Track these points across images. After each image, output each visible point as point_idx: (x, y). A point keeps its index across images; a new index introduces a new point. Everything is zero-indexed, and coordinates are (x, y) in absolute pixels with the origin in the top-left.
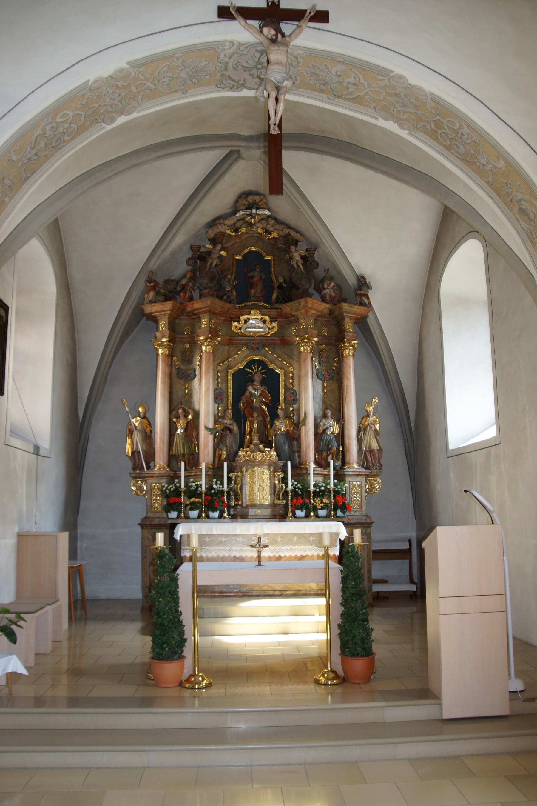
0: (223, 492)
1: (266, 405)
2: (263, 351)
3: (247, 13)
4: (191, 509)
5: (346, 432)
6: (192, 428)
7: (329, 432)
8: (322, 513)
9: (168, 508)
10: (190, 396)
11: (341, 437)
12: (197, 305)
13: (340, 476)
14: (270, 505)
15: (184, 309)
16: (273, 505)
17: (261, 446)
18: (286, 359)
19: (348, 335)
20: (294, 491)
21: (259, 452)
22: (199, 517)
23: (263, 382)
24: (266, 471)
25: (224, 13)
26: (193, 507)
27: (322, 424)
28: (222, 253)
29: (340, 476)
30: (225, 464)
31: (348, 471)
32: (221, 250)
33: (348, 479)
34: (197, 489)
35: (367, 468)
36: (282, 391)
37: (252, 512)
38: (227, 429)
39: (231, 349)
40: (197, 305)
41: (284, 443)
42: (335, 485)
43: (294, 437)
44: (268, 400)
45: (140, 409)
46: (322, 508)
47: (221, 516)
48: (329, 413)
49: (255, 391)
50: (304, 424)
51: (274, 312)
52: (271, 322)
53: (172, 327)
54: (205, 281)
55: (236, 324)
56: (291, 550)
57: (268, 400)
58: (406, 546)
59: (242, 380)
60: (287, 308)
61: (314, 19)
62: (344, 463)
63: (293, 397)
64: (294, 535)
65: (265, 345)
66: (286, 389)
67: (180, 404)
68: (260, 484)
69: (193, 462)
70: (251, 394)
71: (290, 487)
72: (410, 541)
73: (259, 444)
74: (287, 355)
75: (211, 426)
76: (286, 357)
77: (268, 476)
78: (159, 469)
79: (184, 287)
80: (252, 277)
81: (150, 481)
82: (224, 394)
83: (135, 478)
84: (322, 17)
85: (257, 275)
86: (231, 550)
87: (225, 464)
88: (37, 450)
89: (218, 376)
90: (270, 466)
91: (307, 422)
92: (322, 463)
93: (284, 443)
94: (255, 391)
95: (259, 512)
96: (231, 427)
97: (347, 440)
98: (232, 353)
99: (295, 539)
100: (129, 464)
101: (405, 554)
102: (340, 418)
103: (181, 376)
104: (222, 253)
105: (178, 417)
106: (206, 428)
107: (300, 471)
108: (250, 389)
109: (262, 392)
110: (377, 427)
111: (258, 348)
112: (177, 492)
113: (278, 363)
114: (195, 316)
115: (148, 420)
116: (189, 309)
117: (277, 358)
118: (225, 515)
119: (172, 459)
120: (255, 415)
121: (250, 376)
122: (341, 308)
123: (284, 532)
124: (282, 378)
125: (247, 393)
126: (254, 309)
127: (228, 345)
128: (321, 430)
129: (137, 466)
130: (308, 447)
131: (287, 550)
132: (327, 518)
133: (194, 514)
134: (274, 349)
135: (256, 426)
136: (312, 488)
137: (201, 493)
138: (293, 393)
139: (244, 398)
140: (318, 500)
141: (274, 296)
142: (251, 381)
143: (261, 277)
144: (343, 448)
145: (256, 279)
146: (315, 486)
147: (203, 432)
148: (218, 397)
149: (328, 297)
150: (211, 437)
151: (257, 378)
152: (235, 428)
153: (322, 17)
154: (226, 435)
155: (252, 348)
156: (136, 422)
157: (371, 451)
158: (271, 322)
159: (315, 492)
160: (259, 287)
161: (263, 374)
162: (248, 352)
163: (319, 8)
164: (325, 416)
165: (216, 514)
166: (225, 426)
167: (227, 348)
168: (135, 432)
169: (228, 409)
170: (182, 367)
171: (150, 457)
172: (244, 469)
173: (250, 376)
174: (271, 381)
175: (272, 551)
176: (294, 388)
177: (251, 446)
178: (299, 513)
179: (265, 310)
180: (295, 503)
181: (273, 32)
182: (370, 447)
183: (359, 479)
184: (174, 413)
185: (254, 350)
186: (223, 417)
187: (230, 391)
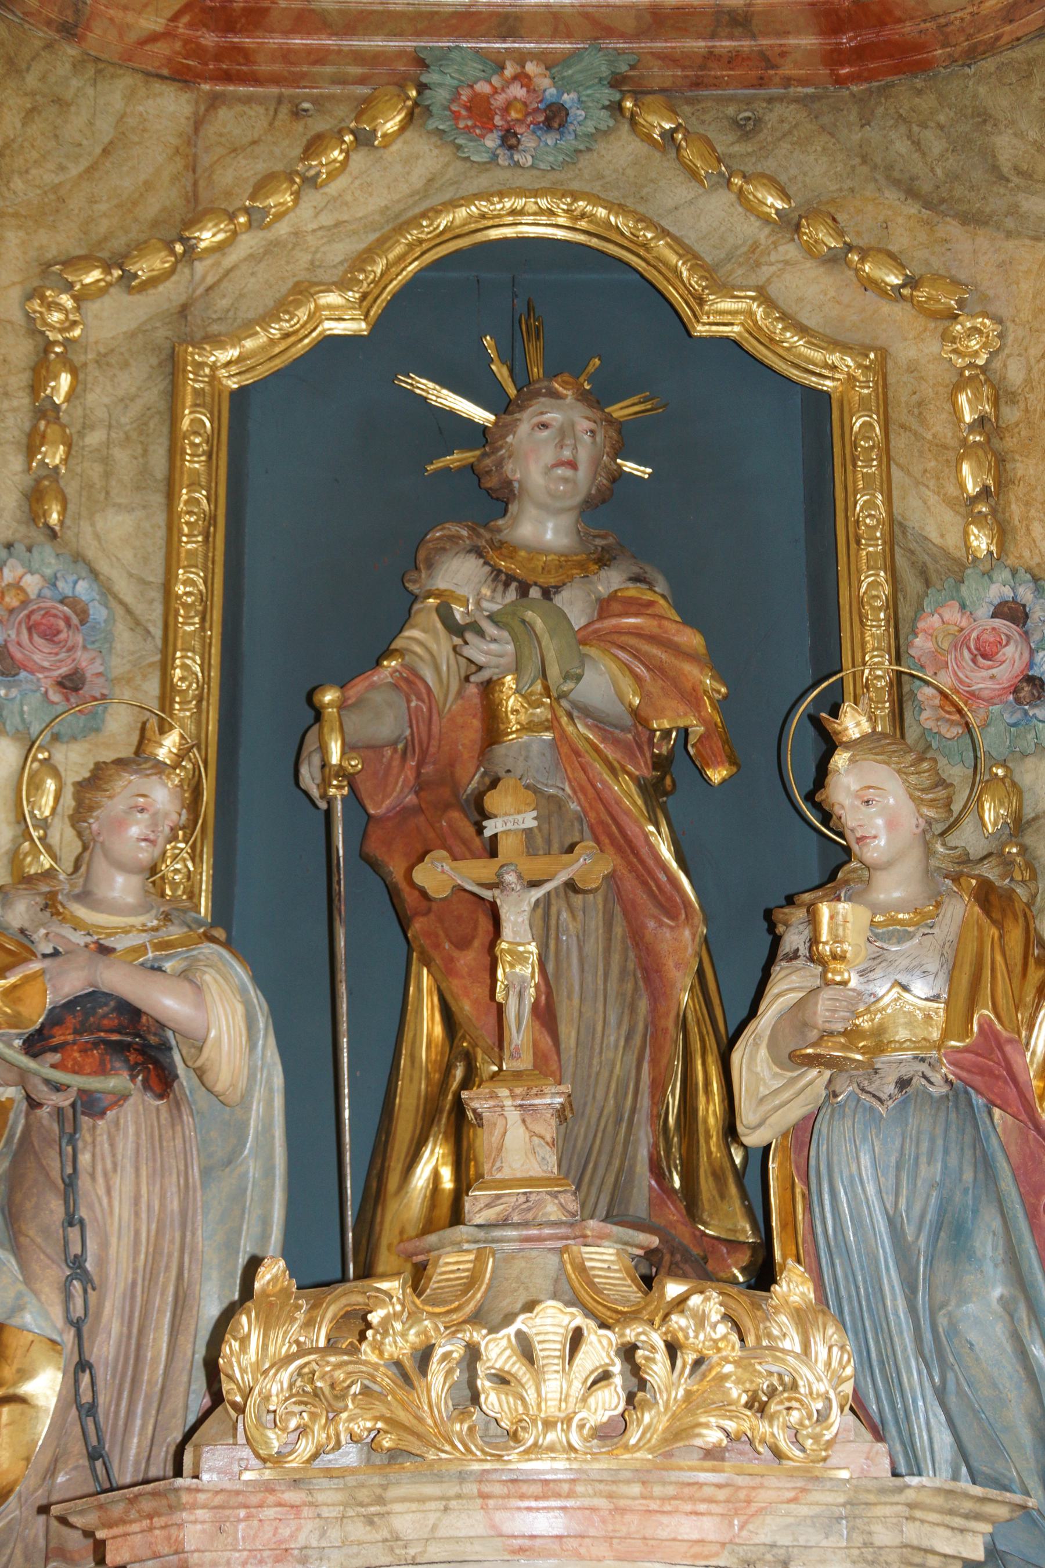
1: (666, 777)
18: (899, 242)
21: (551, 1321)
36: (870, 583)
39: (227, 122)
41: (953, 1233)
44: (692, 698)
49: (523, 651)
57: (692, 698)
63: (1013, 655)
73: (573, 1228)
74: (911, 193)
76: (904, 224)
82: (124, 638)
89: (45, 410)
93: (953, 1233)
94: (523, 651)
96: (167, 1002)
98: (234, 175)
108: (460, 577)
109: (605, 607)
111: (554, 117)
117: (790, 225)
120: (511, 818)
121: (456, 459)
125: (422, 638)
127: (181, 77)
134: (746, 128)
135: (519, 968)
138: (1013, 613)
151: (553, 455)
152: (222, 1018)
154: (90, 1105)
155: (480, 111)
161: (625, 440)
166: (72, 983)
167: (170, 107)
169: (140, 758)
173: (456, 459)
176: (1023, 553)
177: (452, 1263)
185: (509, 140)
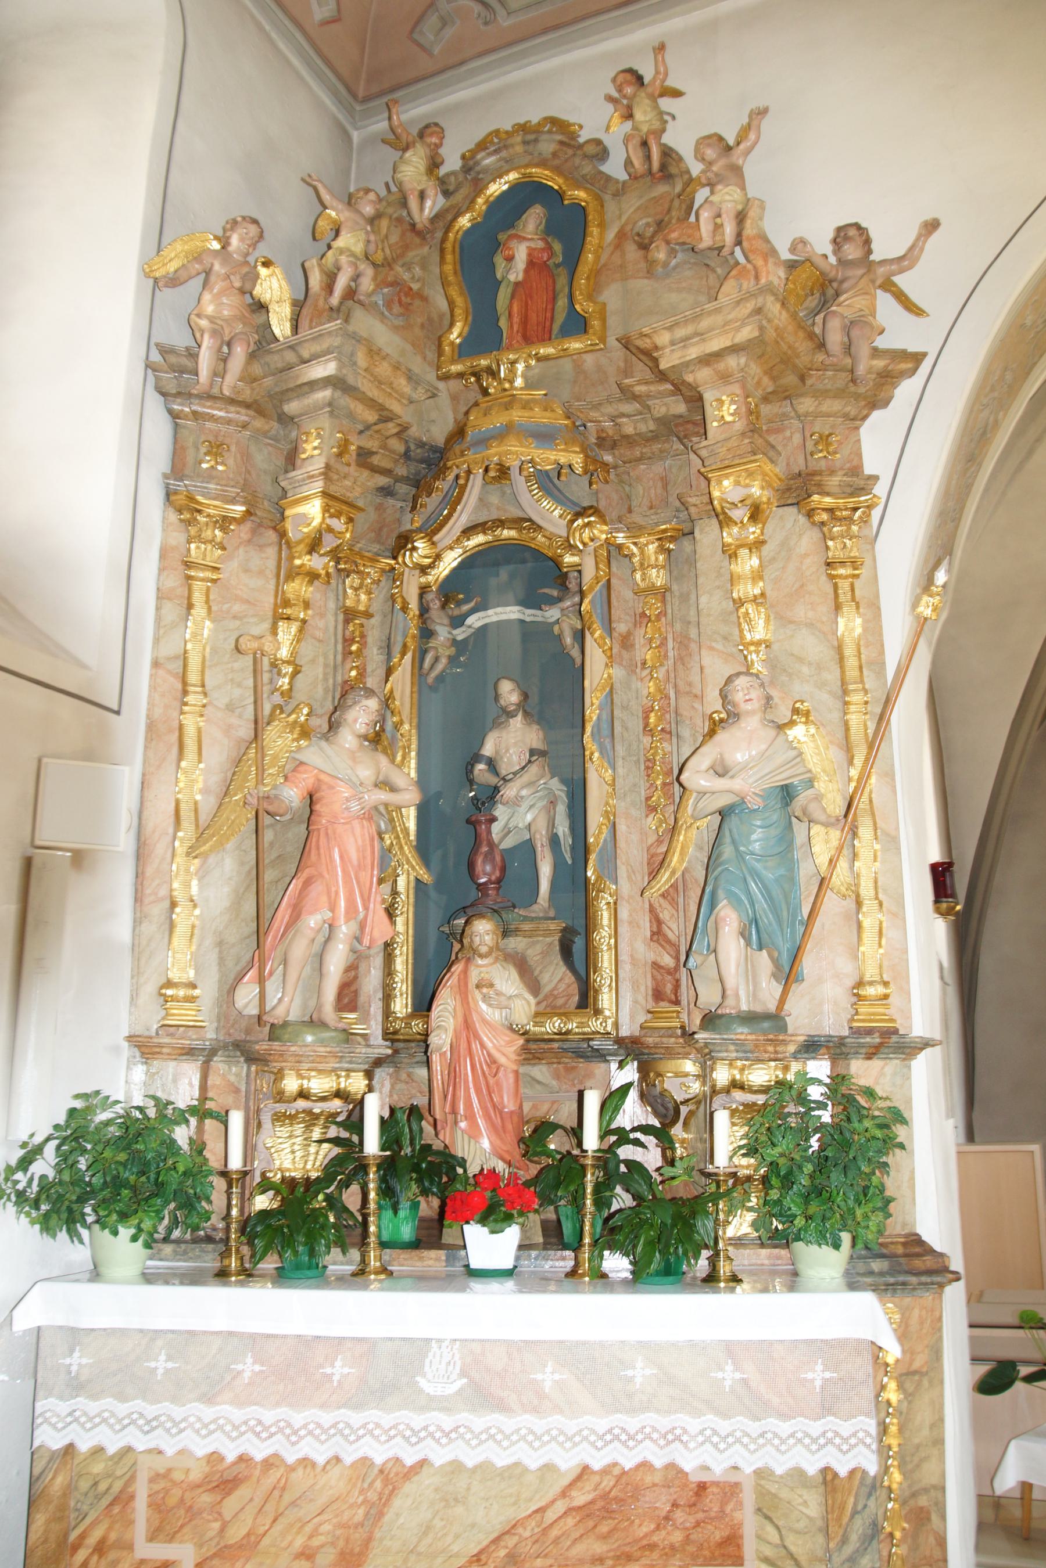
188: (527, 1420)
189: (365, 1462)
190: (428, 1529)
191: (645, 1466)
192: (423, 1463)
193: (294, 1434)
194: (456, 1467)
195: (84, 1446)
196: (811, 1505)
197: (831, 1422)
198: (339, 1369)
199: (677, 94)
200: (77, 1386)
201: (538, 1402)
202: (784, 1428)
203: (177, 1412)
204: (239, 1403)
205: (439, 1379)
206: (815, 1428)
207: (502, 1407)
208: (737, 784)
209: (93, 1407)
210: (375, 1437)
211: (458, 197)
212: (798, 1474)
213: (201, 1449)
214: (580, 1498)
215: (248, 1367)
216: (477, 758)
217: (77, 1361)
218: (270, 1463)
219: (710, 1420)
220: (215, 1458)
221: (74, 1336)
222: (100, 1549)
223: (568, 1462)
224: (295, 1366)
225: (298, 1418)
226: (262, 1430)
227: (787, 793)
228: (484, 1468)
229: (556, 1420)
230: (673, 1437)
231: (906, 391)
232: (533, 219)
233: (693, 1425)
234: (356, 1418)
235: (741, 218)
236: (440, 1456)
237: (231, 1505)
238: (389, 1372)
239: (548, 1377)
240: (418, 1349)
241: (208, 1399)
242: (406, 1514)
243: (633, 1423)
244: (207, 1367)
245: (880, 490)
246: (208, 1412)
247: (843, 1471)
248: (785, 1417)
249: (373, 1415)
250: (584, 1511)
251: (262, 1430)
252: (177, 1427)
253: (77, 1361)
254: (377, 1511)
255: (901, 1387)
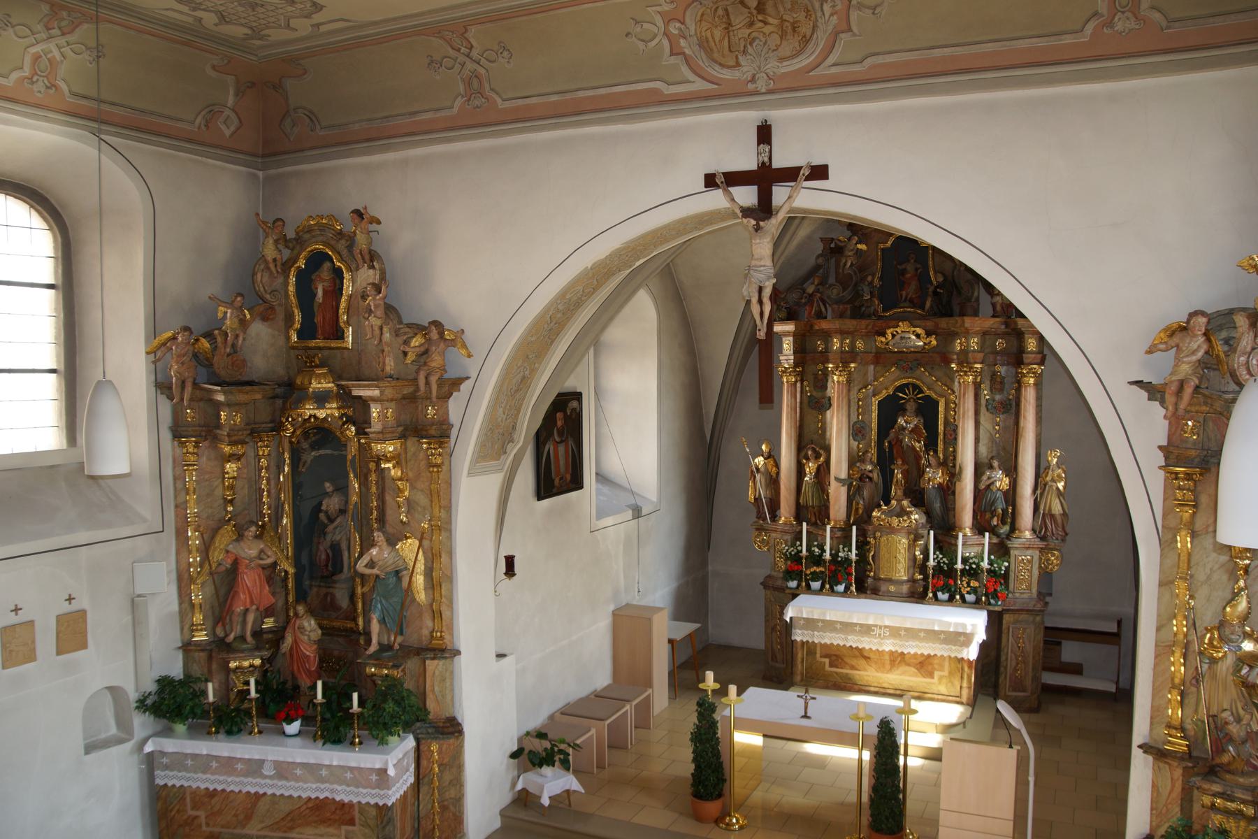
0: (848, 560)
2: (918, 372)
3: (734, 179)
4: (814, 580)
5: (1019, 489)
6: (823, 472)
7: (994, 489)
8: (970, 598)
9: (789, 574)
10: (824, 429)
11: (1011, 496)
12: (824, 325)
13: (1001, 550)
14: (908, 581)
15: (812, 326)
16: (912, 581)
17: (905, 503)
19: (1027, 358)
20: (938, 569)
22: (823, 586)
23: (919, 412)
24: (904, 541)
25: (710, 181)
26: (815, 577)
27: (985, 478)
28: (862, 247)
29: (1001, 550)
30: (854, 528)
31: (1014, 543)
32: (860, 242)
33: (1013, 552)
34: (821, 555)
35: (1043, 538)
36: (941, 428)
37: (883, 588)
38: (864, 477)
40: (824, 325)
42: (991, 563)
43: (948, 491)
45: (764, 447)
46: (968, 593)
47: (847, 589)
48: (996, 463)
50: (959, 480)
51: (930, 324)
52: (928, 334)
53: (799, 350)
54: (835, 291)
55: (883, 339)
56: (917, 646)
58: (1112, 628)
59: (891, 409)
60: (944, 323)
61: (808, 178)
62: (1013, 529)
64: (921, 630)
65: (920, 365)
66: (946, 423)
67: (811, 443)
68: (898, 554)
69: (822, 513)
70: (904, 429)
71: (931, 563)
72: (1119, 623)
75: (844, 475)
77: (906, 546)
78: (785, 524)
79: (811, 295)
80: (904, 272)
81: (774, 535)
83: (757, 529)
84: (820, 172)
85: (910, 267)
86: (846, 639)
87: (854, 528)
88: (637, 513)
90: (909, 533)
91: (963, 476)
92: (979, 528)
95: (892, 588)
97: (1018, 500)
99: (922, 634)
100: (754, 510)
101: (1112, 638)
102: (1012, 470)
103: (815, 404)
104: (862, 247)
105: (808, 459)
106: (837, 479)
107: (945, 544)
108: (901, 421)
110: (1061, 485)
112: (797, 558)
113: (938, 389)
114: (826, 336)
115: (773, 456)
116: (817, 327)
118: (853, 588)
119: (800, 513)
122: (1016, 323)
123: (908, 625)
124: (941, 409)
126: (903, 320)
128: (982, 486)
129: (760, 516)
130: (963, 509)
131: (911, 647)
132: (977, 604)
133: (816, 585)
136: (959, 566)
137: (824, 561)
139: (892, 434)
140: (965, 580)
141: (928, 304)
142: (902, 410)
143: (916, 269)
144: (1014, 510)
145: (908, 276)
146: (965, 560)
147: (833, 483)
148: (857, 431)
149: (999, 308)
150: (843, 491)
151: (911, 407)
153: (820, 172)
156: (760, 461)
157: (1052, 516)
158: (928, 334)
159: (962, 571)
160: (913, 286)
162: (898, 373)
163: (815, 163)
164: (991, 467)
165: (841, 588)
168: (758, 477)
170: (814, 394)
171: (774, 505)
172: (878, 534)
174: (928, 410)
175: (894, 644)
178: (943, 596)
179: (918, 322)
180: (935, 583)
181: (753, 222)
182: (1050, 509)
183: (1029, 552)
184: (803, 454)
186: (863, 461)
187: (874, 425)
188: (292, 783)
189: (248, 792)
190: (268, 811)
191: (327, 798)
192: (265, 794)
193: (229, 784)
194: (274, 795)
195: (170, 784)
196: (374, 812)
197: (377, 790)
198: (239, 766)
199: (379, 222)
200: (166, 767)
201: (297, 779)
202: (364, 791)
203: (196, 776)
204: (212, 774)
205: (268, 770)
206: (374, 792)
207: (287, 779)
208: (375, 571)
209: (171, 774)
210: (251, 786)
211: (296, 252)
212: (368, 803)
213: (203, 786)
214: (310, 805)
215: (214, 764)
216: (320, 511)
217: (165, 760)
218: (223, 790)
219: (344, 787)
220: (207, 789)
221: (163, 754)
222: (178, 811)
223: (304, 795)
224: (228, 764)
225: (229, 780)
226: (220, 782)
227: (397, 573)
228: (282, 795)
229: (301, 784)
230: (332, 791)
231: (465, 387)
232: (327, 265)
233: (339, 788)
234: (246, 780)
235: (381, 328)
236: (270, 792)
237: (213, 801)
238: (254, 767)
239: (298, 772)
240: (261, 763)
241: (204, 772)
242: (262, 806)
243: (322, 786)
244: (203, 763)
245: (454, 432)
246: (204, 777)
247: (381, 804)
248: (365, 787)
249: (250, 779)
250: (311, 809)
251: (220, 782)
252: (196, 780)
253: (165, 760)
254: (255, 804)
255: (439, 766)
